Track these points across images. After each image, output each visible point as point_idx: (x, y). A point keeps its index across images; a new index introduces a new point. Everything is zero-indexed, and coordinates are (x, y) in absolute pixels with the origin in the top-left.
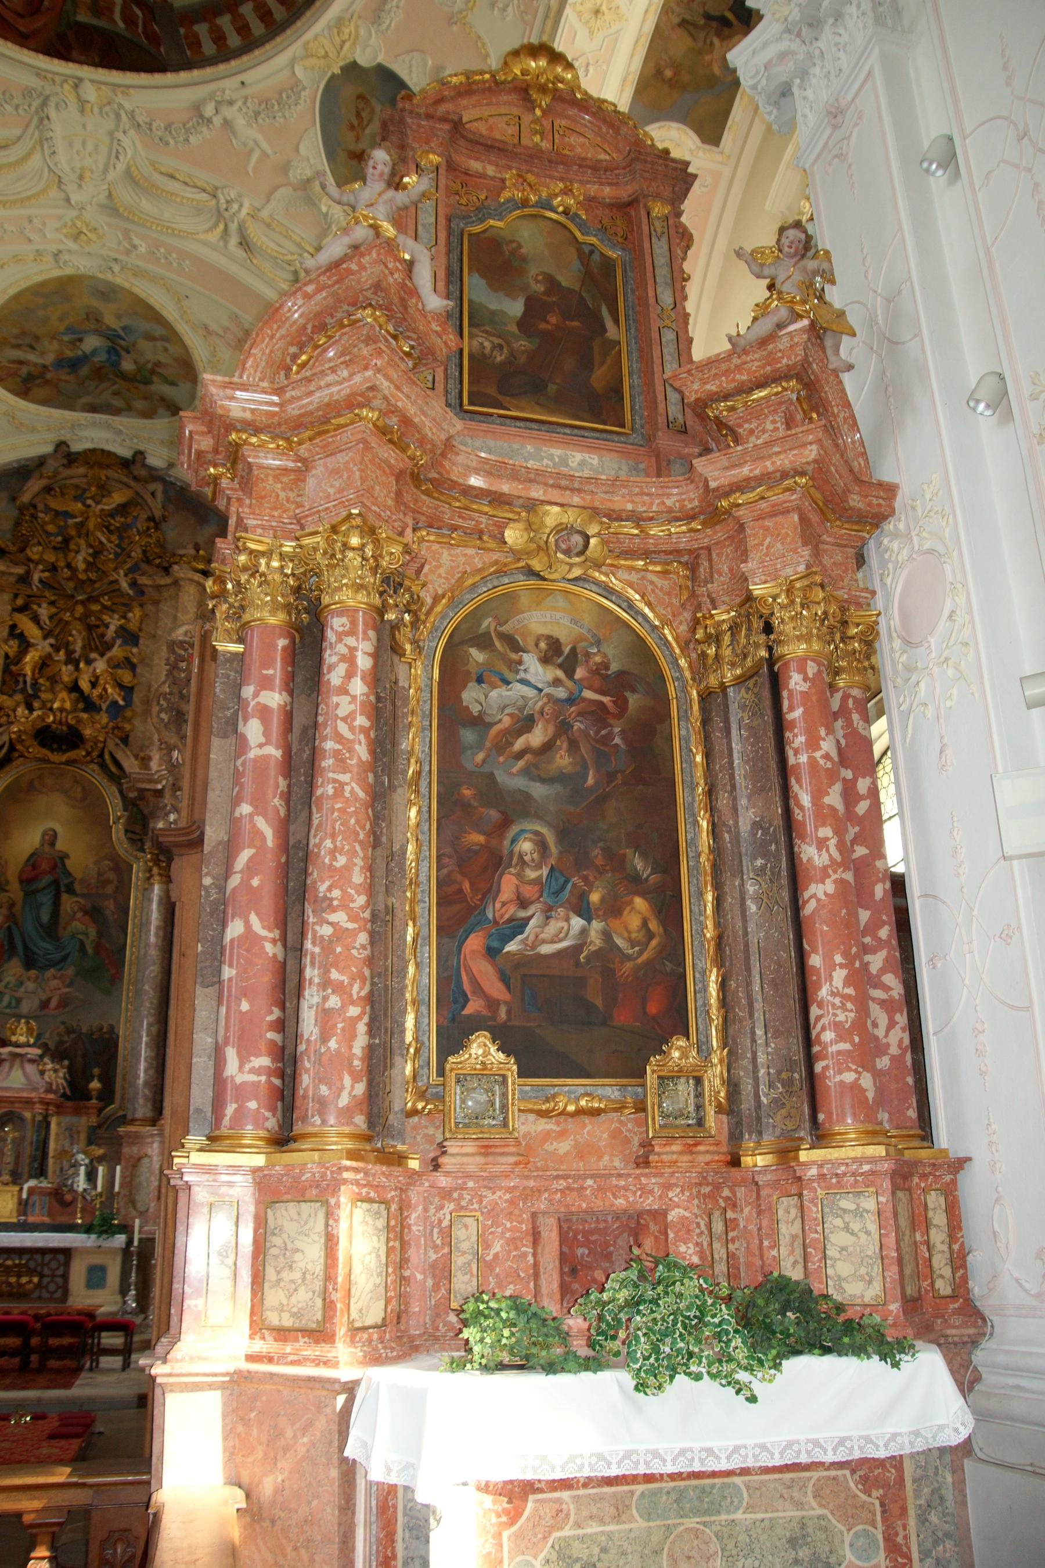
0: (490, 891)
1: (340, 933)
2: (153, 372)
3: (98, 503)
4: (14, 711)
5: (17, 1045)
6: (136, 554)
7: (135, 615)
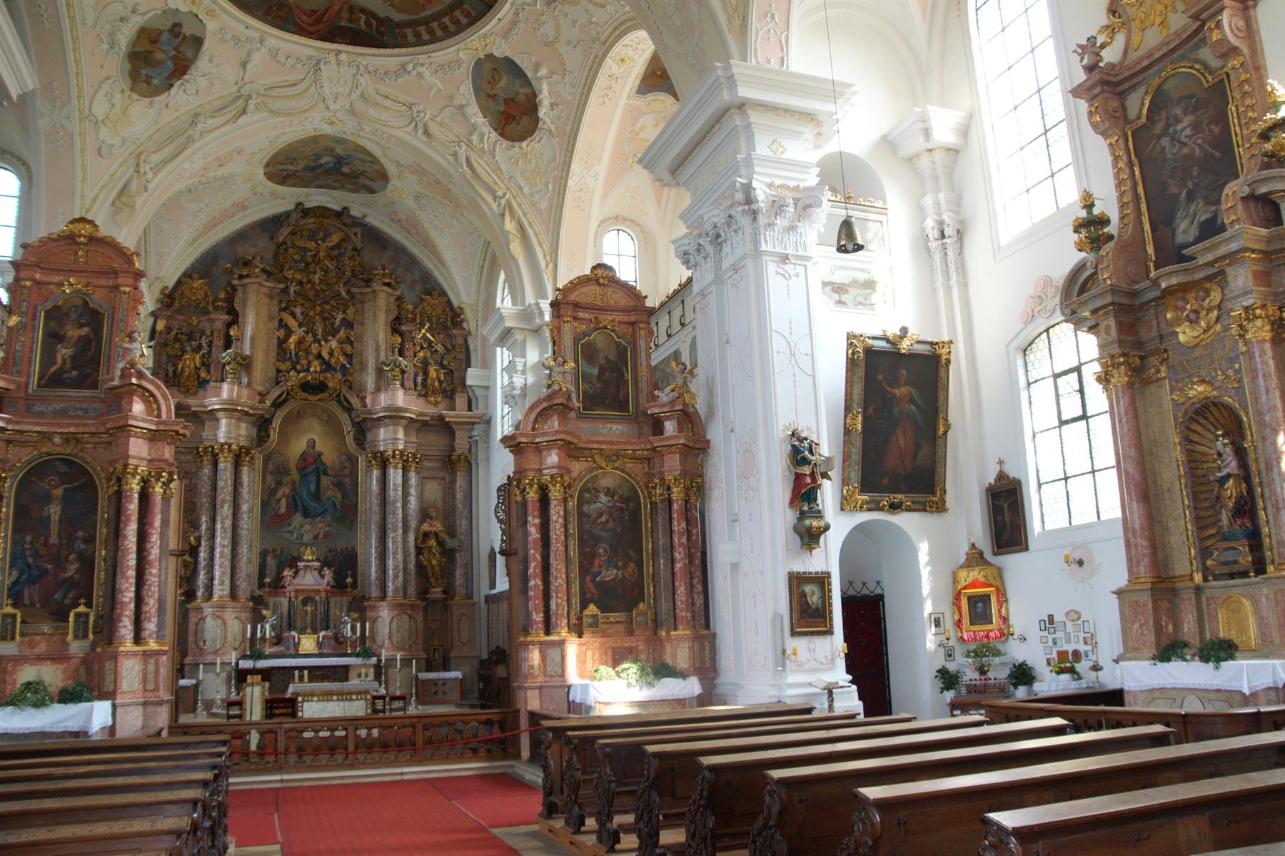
1: (560, 584)
2: (361, 174)
3: (324, 241)
4: (289, 372)
5: (308, 561)
7: (351, 311)
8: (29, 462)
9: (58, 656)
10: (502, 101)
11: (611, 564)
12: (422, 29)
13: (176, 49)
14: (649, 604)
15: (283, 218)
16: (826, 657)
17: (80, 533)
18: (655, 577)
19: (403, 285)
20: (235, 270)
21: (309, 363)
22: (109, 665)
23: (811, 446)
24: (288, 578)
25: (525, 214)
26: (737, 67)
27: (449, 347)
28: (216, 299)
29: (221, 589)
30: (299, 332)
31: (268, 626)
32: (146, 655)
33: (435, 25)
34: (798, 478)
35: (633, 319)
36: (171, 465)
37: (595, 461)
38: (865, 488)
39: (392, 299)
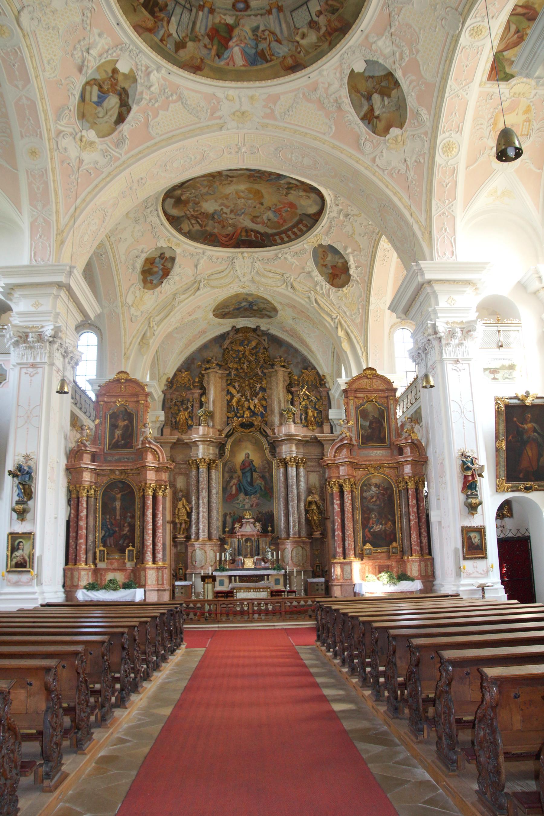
0: (369, 523)
1: (350, 534)
2: (263, 309)
3: (247, 345)
4: (233, 418)
5: (247, 519)
6: (262, 362)
7: (264, 383)
8: (107, 483)
9: (122, 569)
10: (330, 267)
11: (379, 522)
12: (283, 236)
13: (163, 265)
14: (399, 542)
15: (226, 335)
16: (483, 570)
17: (129, 514)
18: (401, 528)
19: (292, 365)
20: (203, 366)
21: (244, 412)
22: (142, 573)
23: (472, 460)
24: (237, 528)
25: (349, 327)
26: (423, 264)
27: (319, 398)
28: (194, 382)
29: (203, 535)
30: (237, 396)
31: (227, 554)
32: (158, 569)
33: (290, 233)
34: (466, 477)
35: (386, 395)
36: (165, 482)
37: (368, 470)
38: (509, 478)
39: (286, 374)
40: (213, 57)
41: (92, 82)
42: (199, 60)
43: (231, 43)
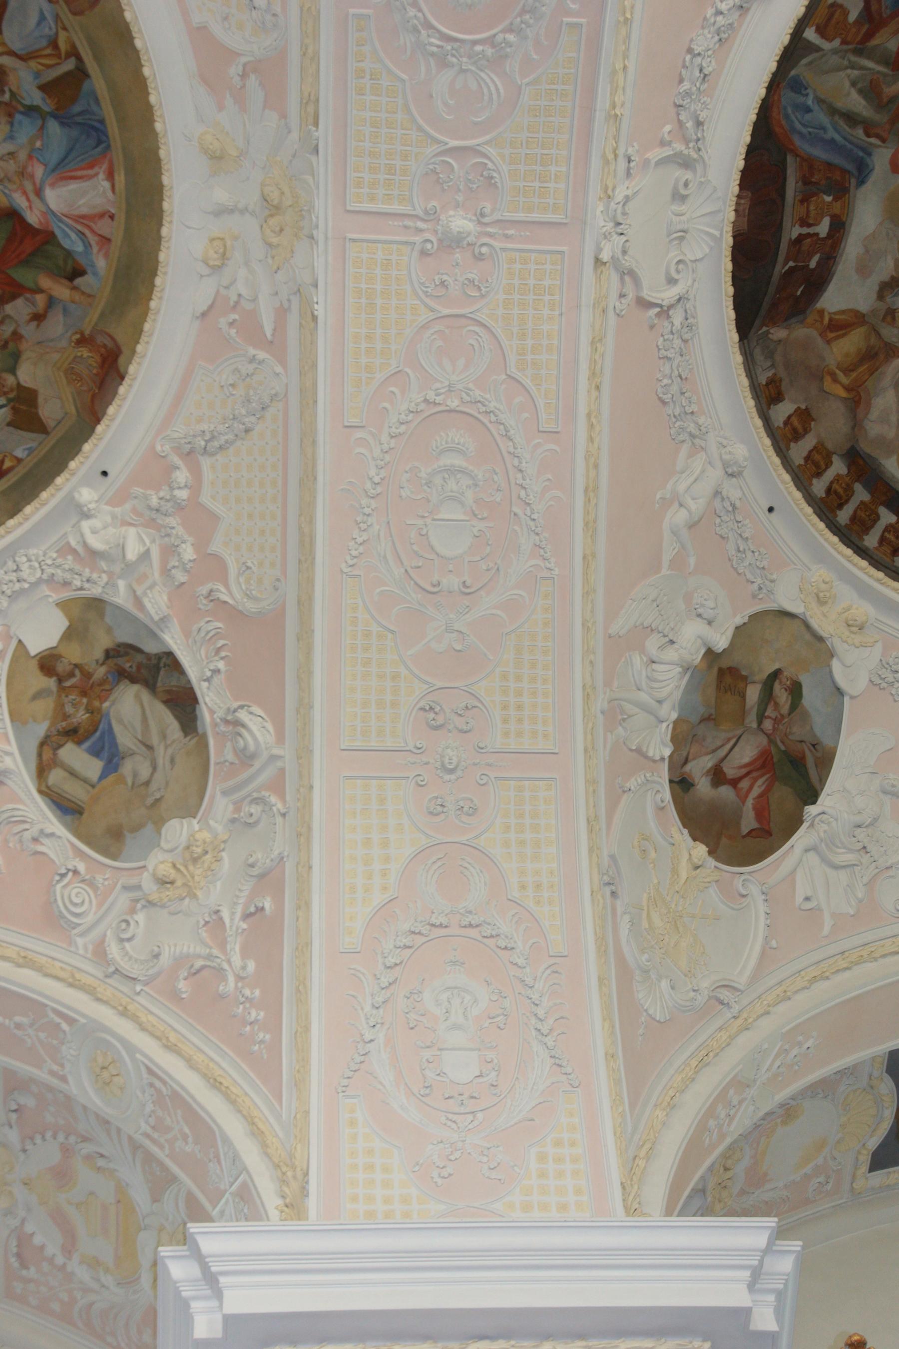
40: (77, 296)
41: (47, 754)
42: (84, 352)
43: (33, 218)
